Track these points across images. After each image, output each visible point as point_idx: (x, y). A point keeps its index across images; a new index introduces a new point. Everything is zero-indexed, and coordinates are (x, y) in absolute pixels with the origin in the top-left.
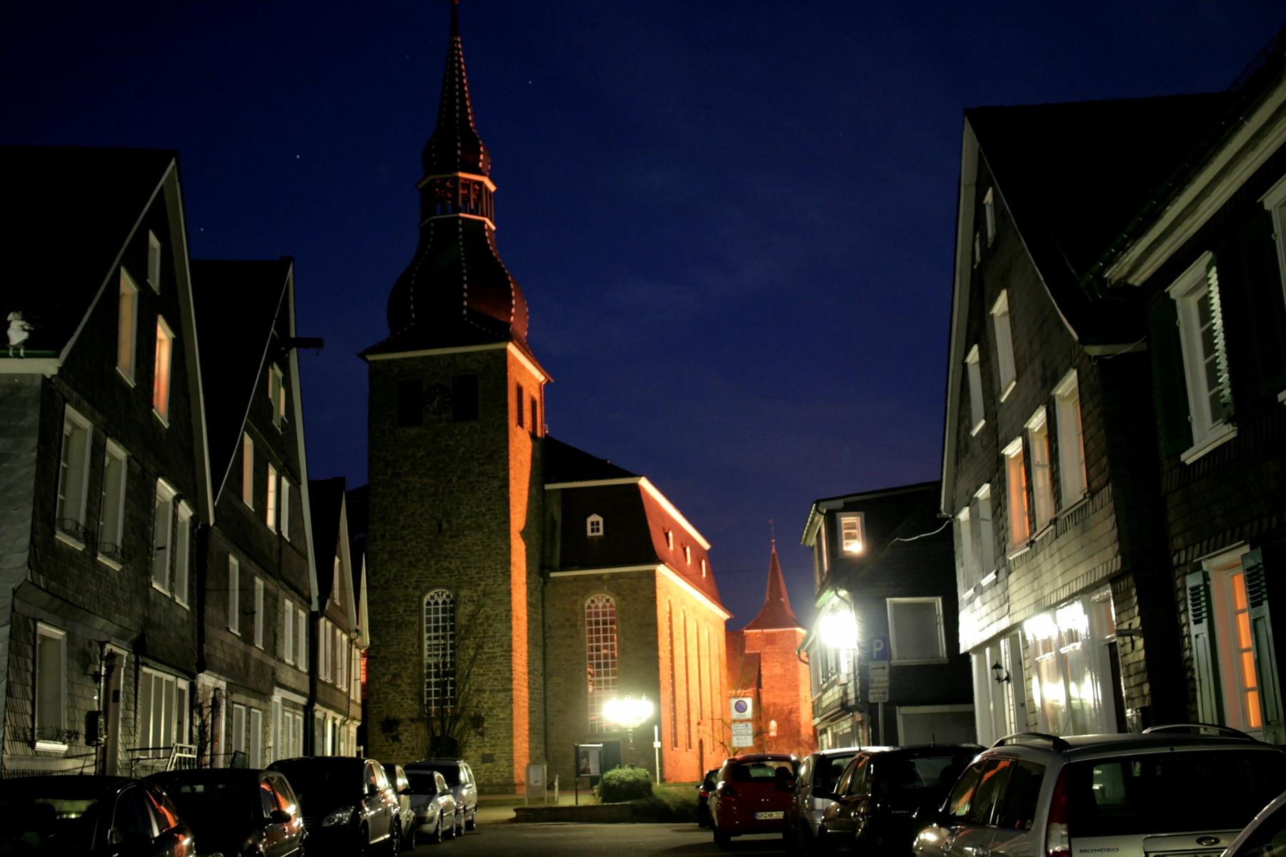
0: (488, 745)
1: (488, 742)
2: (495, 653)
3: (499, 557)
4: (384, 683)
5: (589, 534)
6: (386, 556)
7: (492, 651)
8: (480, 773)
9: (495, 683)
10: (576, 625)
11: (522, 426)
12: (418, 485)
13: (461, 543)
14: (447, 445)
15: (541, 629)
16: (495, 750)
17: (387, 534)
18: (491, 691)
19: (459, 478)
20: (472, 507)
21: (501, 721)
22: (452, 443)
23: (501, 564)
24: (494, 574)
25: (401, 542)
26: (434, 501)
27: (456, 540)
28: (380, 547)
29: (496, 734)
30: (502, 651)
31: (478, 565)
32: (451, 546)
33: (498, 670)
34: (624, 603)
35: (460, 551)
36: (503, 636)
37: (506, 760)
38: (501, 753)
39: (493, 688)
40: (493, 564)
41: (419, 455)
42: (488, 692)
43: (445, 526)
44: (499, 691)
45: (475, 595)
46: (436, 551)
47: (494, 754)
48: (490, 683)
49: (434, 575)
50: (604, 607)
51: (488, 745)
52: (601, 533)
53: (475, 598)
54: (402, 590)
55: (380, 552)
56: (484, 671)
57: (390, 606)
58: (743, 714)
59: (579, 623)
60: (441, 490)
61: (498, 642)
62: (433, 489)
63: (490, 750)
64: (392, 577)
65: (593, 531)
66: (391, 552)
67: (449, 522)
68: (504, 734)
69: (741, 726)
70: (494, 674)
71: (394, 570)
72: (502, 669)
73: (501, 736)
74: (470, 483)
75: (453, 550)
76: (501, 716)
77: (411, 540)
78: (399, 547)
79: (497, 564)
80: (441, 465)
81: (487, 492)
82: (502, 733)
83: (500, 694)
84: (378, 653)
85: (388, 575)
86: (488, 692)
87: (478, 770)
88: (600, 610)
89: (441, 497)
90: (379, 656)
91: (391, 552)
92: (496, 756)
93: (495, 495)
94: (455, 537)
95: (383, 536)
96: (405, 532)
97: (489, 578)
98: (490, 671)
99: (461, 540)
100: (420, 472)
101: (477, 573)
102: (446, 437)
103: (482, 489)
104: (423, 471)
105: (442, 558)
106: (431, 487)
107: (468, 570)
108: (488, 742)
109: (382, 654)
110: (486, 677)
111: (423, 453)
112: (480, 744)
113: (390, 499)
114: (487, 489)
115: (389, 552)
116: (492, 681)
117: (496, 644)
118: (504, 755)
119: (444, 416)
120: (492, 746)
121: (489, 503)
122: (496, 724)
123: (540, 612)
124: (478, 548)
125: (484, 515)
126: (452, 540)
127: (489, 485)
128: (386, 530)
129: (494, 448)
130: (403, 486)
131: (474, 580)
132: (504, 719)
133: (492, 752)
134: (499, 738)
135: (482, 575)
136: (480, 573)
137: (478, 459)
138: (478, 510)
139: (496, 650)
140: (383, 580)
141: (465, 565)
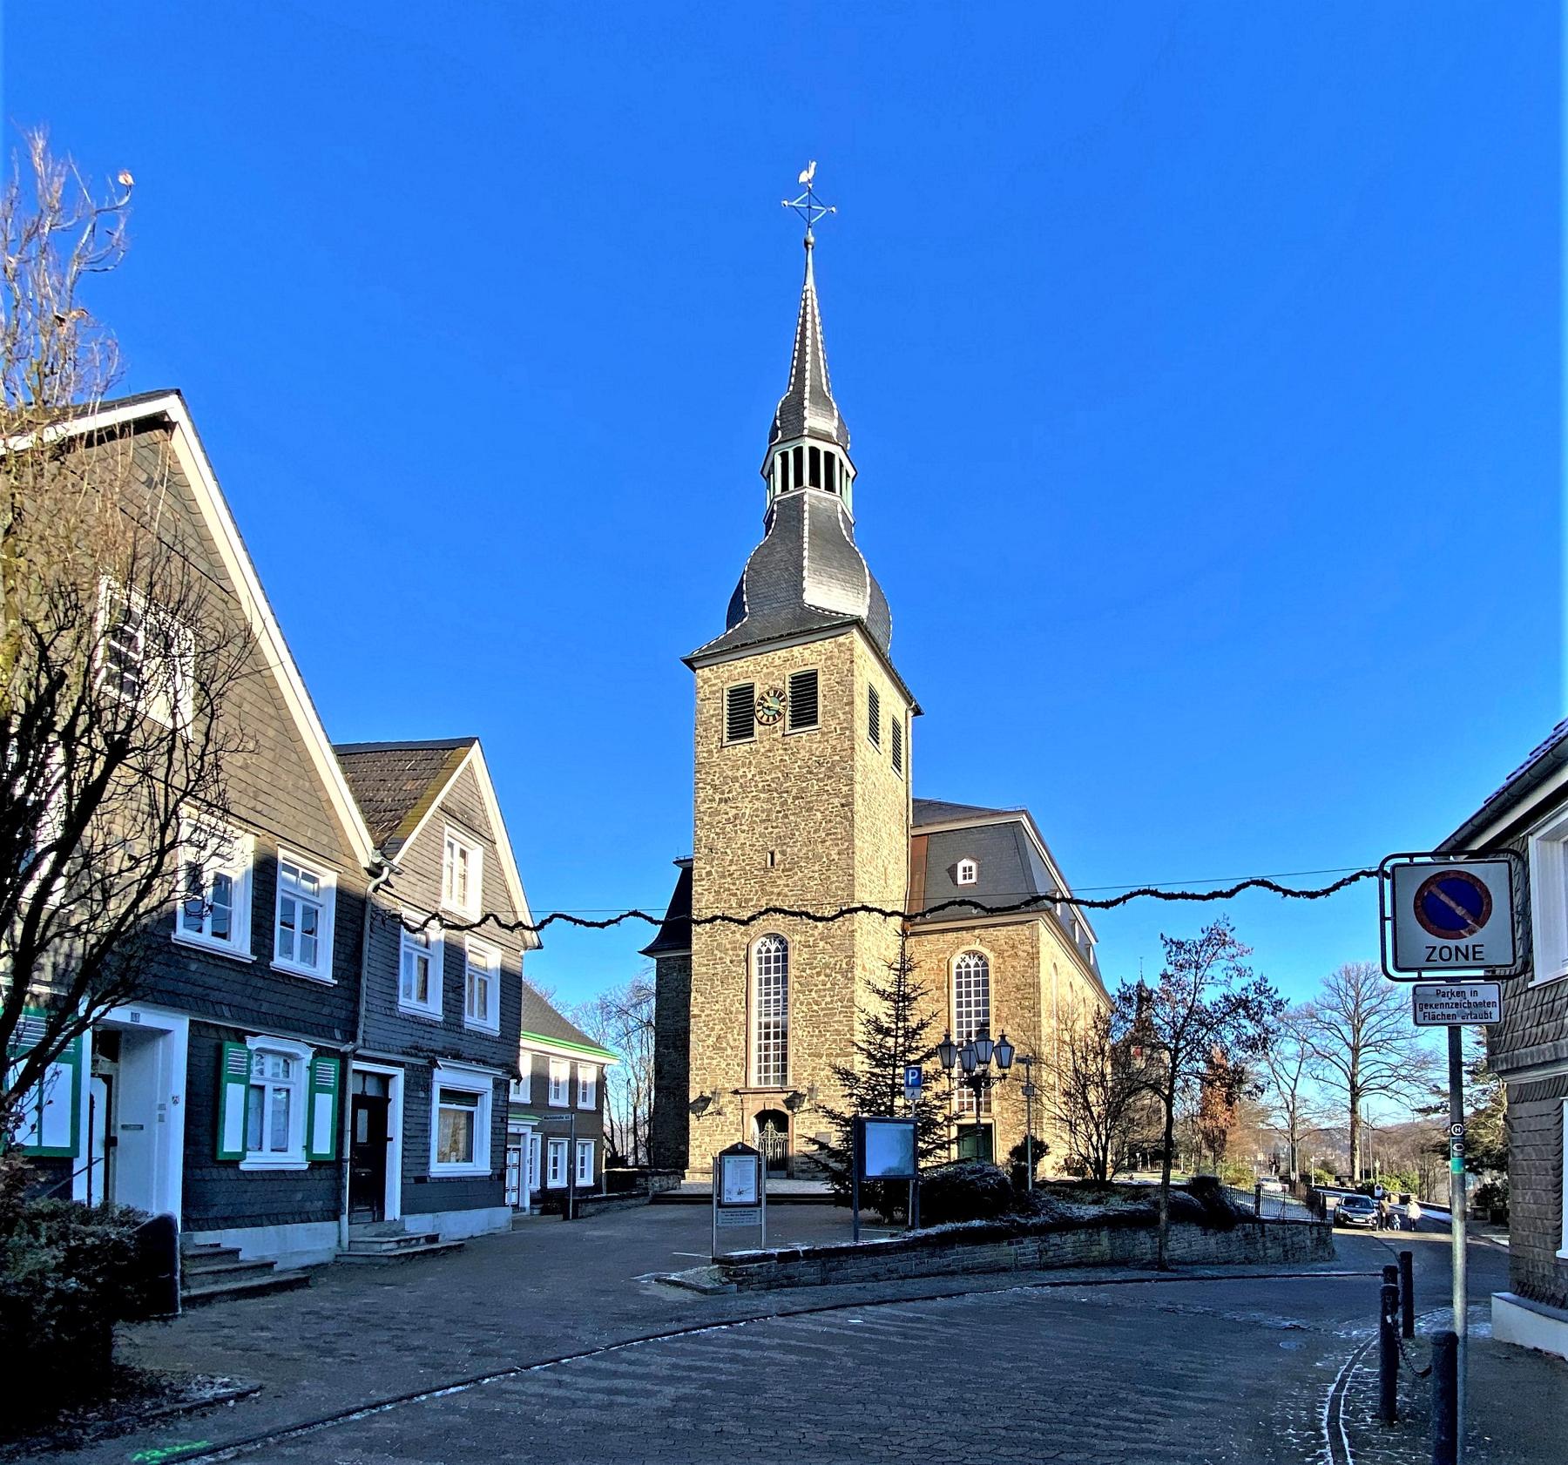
4: (708, 1047)
9: (833, 1046)
12: (748, 812)
13: (796, 878)
20: (809, 832)
28: (706, 887)
31: (814, 902)
42: (824, 1057)
43: (778, 857)
45: (811, 939)
46: (768, 889)
48: (827, 1046)
56: (820, 1031)
67: (783, 853)
75: (788, 886)
78: (726, 885)
80: (774, 785)
81: (827, 812)
84: (703, 1011)
89: (774, 824)
90: (703, 1015)
91: (717, 893)
94: (790, 870)
96: (734, 867)
102: (781, 752)
103: (822, 809)
104: (754, 794)
106: (763, 812)
109: (707, 1012)
111: (753, 773)
112: (814, 1121)
113: (718, 830)
124: (816, 882)
125: (823, 842)
126: (786, 873)
128: (713, 867)
129: (837, 758)
137: (817, 774)
141: (800, 903)
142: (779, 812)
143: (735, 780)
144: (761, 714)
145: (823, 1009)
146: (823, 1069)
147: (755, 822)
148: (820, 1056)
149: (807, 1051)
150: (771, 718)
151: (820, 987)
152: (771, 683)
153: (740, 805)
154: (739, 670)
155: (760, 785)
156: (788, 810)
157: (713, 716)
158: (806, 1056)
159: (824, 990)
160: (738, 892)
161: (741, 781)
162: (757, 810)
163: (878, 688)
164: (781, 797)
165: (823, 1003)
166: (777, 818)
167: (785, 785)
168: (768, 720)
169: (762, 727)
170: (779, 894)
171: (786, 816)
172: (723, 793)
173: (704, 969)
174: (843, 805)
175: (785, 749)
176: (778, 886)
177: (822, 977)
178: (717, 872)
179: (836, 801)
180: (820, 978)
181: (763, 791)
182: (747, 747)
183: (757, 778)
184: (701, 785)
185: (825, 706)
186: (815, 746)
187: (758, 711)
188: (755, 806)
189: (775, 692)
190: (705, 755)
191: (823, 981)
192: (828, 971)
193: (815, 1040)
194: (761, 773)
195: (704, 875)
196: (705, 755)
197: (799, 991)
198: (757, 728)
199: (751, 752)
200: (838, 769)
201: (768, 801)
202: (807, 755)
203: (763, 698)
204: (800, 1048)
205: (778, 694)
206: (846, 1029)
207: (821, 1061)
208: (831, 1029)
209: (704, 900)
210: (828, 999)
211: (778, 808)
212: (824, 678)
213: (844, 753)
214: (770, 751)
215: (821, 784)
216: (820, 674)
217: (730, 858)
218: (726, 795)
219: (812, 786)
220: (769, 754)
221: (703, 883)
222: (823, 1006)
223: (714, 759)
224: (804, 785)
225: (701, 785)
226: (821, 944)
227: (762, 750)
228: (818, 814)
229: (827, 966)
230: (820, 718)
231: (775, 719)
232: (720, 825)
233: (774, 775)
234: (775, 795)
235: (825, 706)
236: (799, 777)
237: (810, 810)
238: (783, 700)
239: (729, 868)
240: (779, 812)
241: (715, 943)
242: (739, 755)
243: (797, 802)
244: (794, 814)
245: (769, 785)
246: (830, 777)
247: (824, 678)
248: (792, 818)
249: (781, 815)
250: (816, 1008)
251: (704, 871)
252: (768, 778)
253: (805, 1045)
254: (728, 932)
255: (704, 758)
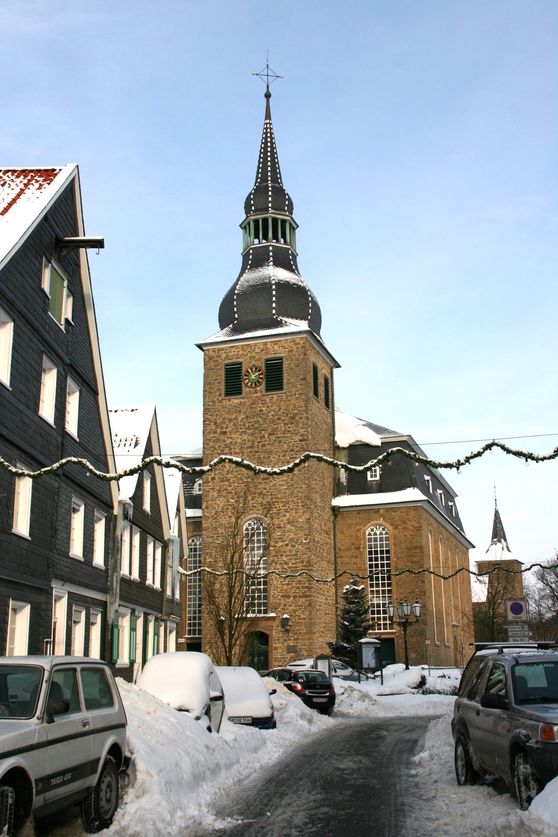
0: (292, 639)
1: (292, 637)
2: (298, 567)
3: (300, 494)
5: (369, 479)
6: (215, 494)
7: (295, 566)
8: (286, 661)
9: (297, 591)
10: (360, 548)
11: (317, 396)
12: (239, 441)
13: (271, 484)
14: (261, 410)
15: (333, 551)
16: (297, 643)
17: (217, 478)
18: (295, 597)
19: (270, 434)
21: (302, 620)
22: (264, 409)
23: (301, 498)
24: (296, 507)
25: (227, 483)
26: (251, 452)
27: (267, 481)
28: (212, 487)
29: (298, 630)
30: (302, 566)
31: (284, 500)
32: (263, 486)
33: (300, 581)
34: (397, 531)
35: (271, 489)
36: (303, 554)
37: (306, 651)
38: (302, 645)
39: (296, 594)
40: (295, 499)
41: (240, 419)
42: (292, 598)
44: (300, 597)
45: (282, 523)
46: (253, 490)
47: (297, 646)
48: (293, 591)
49: (251, 508)
50: (381, 534)
51: (292, 639)
52: (378, 478)
53: (282, 526)
54: (228, 519)
55: (212, 491)
56: (289, 581)
57: (219, 531)
58: (519, 616)
59: (362, 546)
60: (256, 444)
61: (299, 559)
62: (250, 443)
63: (294, 643)
64: (220, 510)
65: (372, 476)
66: (219, 491)
68: (305, 631)
69: (517, 628)
70: (296, 584)
71: (221, 505)
72: (302, 580)
73: (302, 632)
74: (278, 438)
75: (266, 489)
76: (302, 616)
77: (234, 482)
78: (225, 487)
79: (298, 499)
80: (256, 425)
81: (290, 444)
82: (303, 630)
83: (301, 599)
85: (217, 508)
86: (292, 598)
87: (284, 658)
88: (378, 536)
89: (256, 450)
91: (219, 491)
92: (298, 648)
93: (297, 447)
95: (213, 479)
96: (230, 475)
97: (292, 510)
98: (294, 581)
99: (271, 481)
100: (240, 431)
101: (283, 506)
102: (260, 405)
103: (287, 442)
104: (243, 430)
105: (257, 495)
106: (249, 441)
107: (276, 504)
108: (292, 637)
110: (291, 586)
111: (242, 417)
112: (286, 638)
113: (219, 451)
114: (290, 442)
115: (217, 490)
116: (295, 589)
117: (298, 561)
118: (304, 647)
119: (258, 389)
120: (296, 639)
121: (292, 453)
122: (298, 623)
123: (332, 537)
126: (265, 481)
127: (291, 439)
128: (216, 474)
129: (297, 411)
130: (229, 441)
131: (281, 511)
132: (304, 619)
133: (296, 645)
134: (300, 634)
135: (286, 508)
136: (286, 506)
137: (283, 421)
138: (284, 458)
139: (298, 565)
140: (214, 512)
142: (259, 442)
143: (230, 420)
144: (247, 381)
145: (289, 567)
146: (291, 606)
147: (243, 448)
148: (289, 597)
149: (281, 594)
150: (254, 385)
151: (288, 553)
152: (254, 362)
153: (233, 436)
154: (232, 353)
155: (247, 425)
156: (266, 441)
157: (215, 380)
158: (280, 597)
159: (291, 555)
160: (233, 492)
161: (235, 421)
162: (245, 440)
163: (316, 362)
164: (261, 433)
165: (290, 564)
166: (258, 446)
167: (263, 426)
168: (252, 385)
169: (248, 389)
170: (259, 494)
171: (264, 445)
172: (222, 428)
173: (210, 540)
174: (300, 441)
175: (262, 404)
176: (260, 489)
177: (290, 547)
178: (219, 478)
179: (297, 438)
180: (288, 548)
181: (249, 428)
182: (238, 401)
183: (244, 420)
184: (208, 422)
185: (288, 380)
186: (282, 403)
187: (245, 379)
188: (244, 438)
189: (256, 369)
190: (211, 404)
191: (290, 550)
192: (293, 543)
193: (285, 587)
194: (247, 417)
195: (210, 479)
196: (211, 404)
197: (274, 556)
198: (245, 390)
199: (240, 404)
200: (297, 418)
201: (252, 435)
202: (277, 408)
203: (248, 372)
204: (276, 592)
205: (258, 369)
206: (306, 580)
207: (289, 600)
208: (295, 580)
209: (211, 495)
210: (294, 561)
211: (259, 440)
212: (287, 362)
213: (301, 409)
214: (252, 404)
215: (287, 427)
216: (284, 359)
217: (227, 469)
218: (225, 430)
219: (281, 428)
220: (253, 406)
221: (210, 484)
222: (290, 565)
223: (216, 406)
224: (276, 426)
225: (208, 422)
226: (289, 526)
227: (248, 403)
228: (285, 445)
229: (292, 540)
230: (285, 386)
231: (256, 384)
232: (221, 448)
233: (255, 419)
234: (257, 431)
235: (288, 380)
236: (273, 421)
237: (280, 442)
238: (261, 374)
239: (227, 476)
240: (259, 442)
241: (218, 523)
242: (233, 405)
243: (271, 437)
244: (269, 444)
245: (252, 425)
246: (292, 423)
247: (287, 362)
248: (268, 447)
249: (260, 444)
250: (286, 566)
251: (210, 477)
252: (252, 421)
253: (279, 590)
254: (226, 517)
255: (209, 405)
